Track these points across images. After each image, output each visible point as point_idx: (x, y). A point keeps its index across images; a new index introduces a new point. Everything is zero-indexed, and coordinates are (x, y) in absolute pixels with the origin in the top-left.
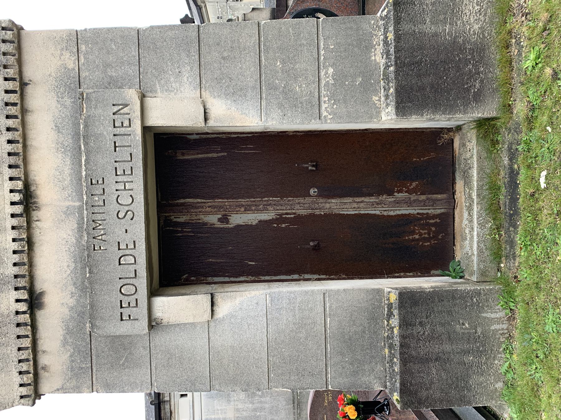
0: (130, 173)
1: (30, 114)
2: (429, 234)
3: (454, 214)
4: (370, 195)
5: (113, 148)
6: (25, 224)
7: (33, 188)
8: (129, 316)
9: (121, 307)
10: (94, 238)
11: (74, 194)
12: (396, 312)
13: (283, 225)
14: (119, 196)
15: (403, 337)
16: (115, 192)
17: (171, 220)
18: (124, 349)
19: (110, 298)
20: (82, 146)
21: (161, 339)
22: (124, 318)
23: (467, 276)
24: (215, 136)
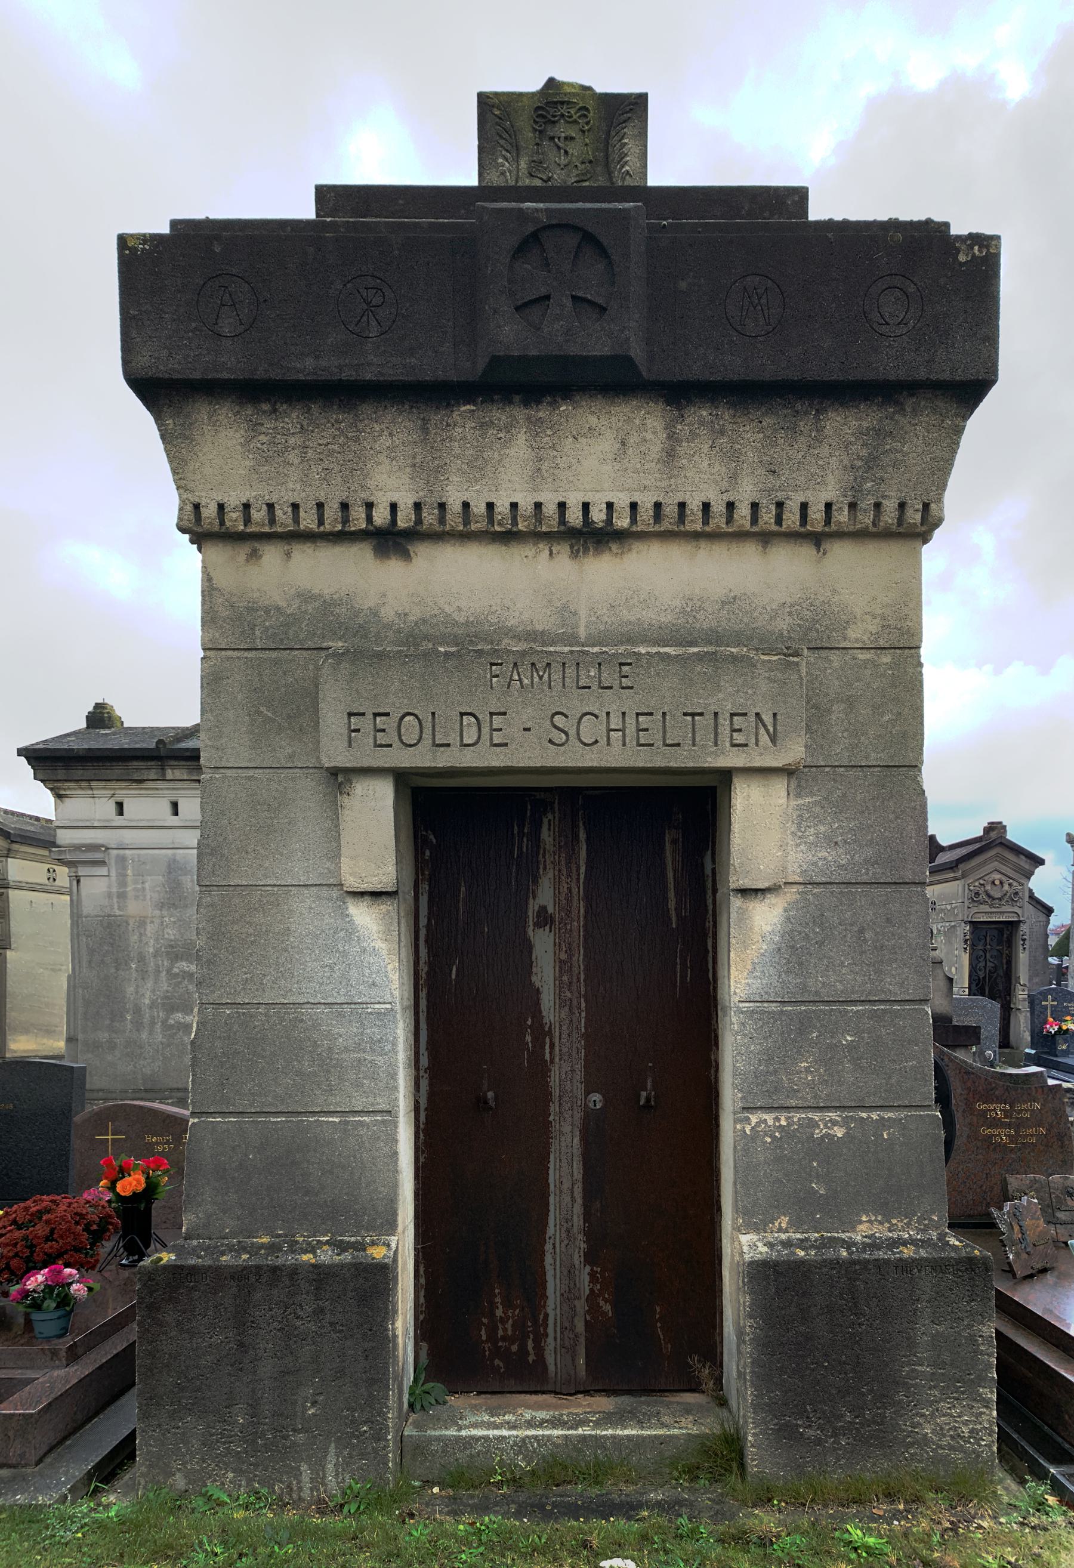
0: (642, 741)
1: (760, 548)
2: (503, 1339)
3: (544, 1393)
4: (587, 1215)
5: (690, 710)
6: (544, 529)
7: (614, 547)
8: (358, 730)
9: (376, 715)
10: (515, 664)
11: (602, 628)
12: (347, 1257)
13: (528, 1038)
14: (596, 717)
15: (294, 1271)
16: (605, 711)
18: (289, 717)
20: (696, 650)
21: (308, 792)
22: (353, 719)
23: (413, 1417)
24: (711, 907)
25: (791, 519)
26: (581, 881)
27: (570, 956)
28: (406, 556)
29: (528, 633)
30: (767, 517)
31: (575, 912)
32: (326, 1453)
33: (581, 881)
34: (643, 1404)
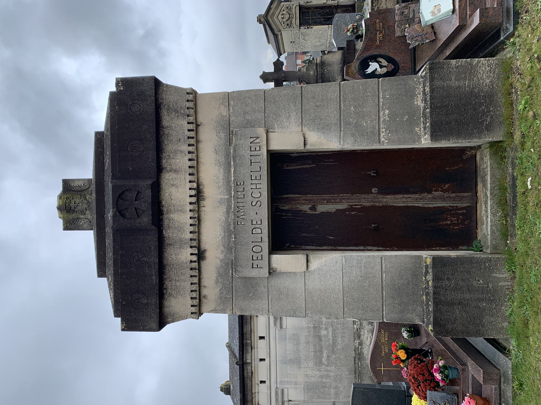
2: (458, 221)
3: (476, 207)
4: (415, 193)
7: (201, 187)
13: (353, 213)
19: (246, 254)
21: (276, 282)
23: (484, 250)
25: (192, 134)
27: (325, 199)
28: (205, 251)
29: (227, 213)
30: (192, 141)
31: (311, 198)
32: (495, 277)
34: (480, 174)
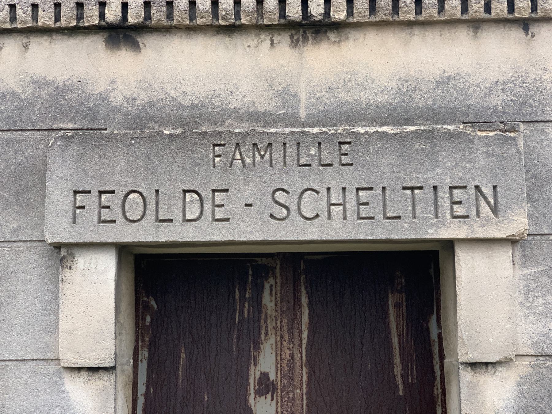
0: (363, 215)
1: (471, 33)
5: (409, 185)
6: (266, 22)
7: (332, 36)
8: (83, 207)
9: (101, 193)
10: (237, 145)
11: (322, 108)
14: (317, 192)
16: (325, 187)
17: (267, 278)
18: (17, 192)
19: (119, 171)
20: (413, 128)
21: (30, 265)
22: (78, 197)
26: (304, 346)
29: (250, 114)
31: (297, 378)
33: (304, 346)
